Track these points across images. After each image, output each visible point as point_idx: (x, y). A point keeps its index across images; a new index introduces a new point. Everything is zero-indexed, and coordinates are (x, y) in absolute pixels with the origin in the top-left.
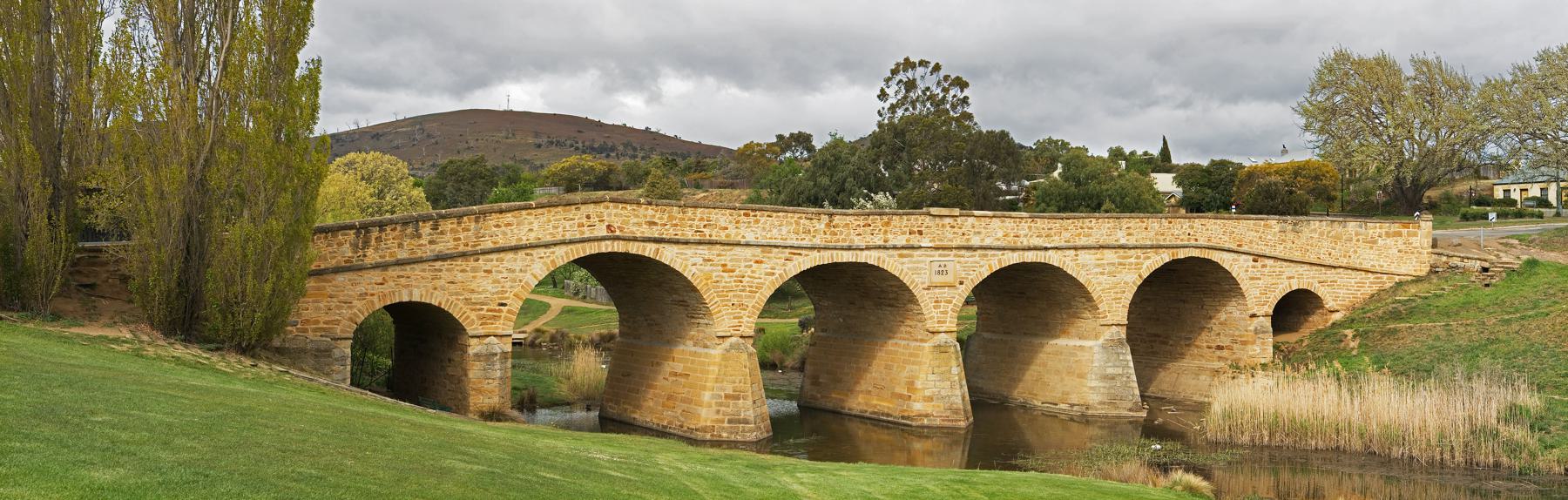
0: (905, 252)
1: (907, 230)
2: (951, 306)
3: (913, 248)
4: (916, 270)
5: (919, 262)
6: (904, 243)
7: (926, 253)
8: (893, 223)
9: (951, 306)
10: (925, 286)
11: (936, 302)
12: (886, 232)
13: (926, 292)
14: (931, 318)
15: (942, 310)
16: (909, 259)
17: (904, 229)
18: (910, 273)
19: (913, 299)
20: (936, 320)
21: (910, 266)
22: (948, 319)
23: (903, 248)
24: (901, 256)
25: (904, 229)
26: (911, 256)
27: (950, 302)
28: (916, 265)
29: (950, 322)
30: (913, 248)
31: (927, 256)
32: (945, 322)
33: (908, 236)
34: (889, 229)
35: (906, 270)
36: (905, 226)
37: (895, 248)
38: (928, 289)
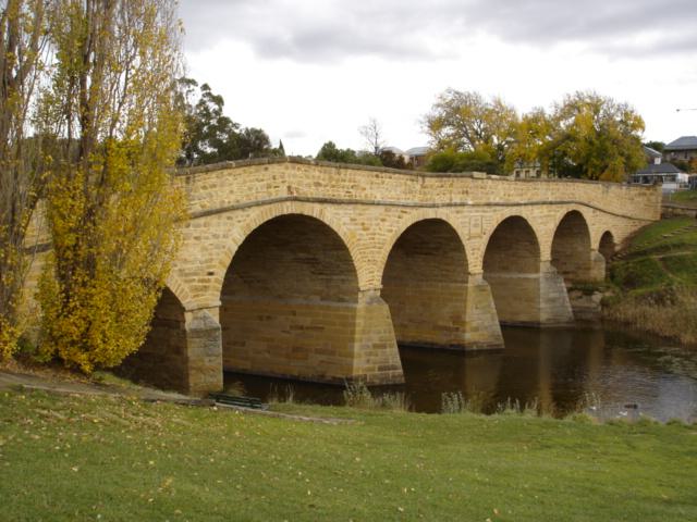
24: (458, 212)
26: (462, 212)
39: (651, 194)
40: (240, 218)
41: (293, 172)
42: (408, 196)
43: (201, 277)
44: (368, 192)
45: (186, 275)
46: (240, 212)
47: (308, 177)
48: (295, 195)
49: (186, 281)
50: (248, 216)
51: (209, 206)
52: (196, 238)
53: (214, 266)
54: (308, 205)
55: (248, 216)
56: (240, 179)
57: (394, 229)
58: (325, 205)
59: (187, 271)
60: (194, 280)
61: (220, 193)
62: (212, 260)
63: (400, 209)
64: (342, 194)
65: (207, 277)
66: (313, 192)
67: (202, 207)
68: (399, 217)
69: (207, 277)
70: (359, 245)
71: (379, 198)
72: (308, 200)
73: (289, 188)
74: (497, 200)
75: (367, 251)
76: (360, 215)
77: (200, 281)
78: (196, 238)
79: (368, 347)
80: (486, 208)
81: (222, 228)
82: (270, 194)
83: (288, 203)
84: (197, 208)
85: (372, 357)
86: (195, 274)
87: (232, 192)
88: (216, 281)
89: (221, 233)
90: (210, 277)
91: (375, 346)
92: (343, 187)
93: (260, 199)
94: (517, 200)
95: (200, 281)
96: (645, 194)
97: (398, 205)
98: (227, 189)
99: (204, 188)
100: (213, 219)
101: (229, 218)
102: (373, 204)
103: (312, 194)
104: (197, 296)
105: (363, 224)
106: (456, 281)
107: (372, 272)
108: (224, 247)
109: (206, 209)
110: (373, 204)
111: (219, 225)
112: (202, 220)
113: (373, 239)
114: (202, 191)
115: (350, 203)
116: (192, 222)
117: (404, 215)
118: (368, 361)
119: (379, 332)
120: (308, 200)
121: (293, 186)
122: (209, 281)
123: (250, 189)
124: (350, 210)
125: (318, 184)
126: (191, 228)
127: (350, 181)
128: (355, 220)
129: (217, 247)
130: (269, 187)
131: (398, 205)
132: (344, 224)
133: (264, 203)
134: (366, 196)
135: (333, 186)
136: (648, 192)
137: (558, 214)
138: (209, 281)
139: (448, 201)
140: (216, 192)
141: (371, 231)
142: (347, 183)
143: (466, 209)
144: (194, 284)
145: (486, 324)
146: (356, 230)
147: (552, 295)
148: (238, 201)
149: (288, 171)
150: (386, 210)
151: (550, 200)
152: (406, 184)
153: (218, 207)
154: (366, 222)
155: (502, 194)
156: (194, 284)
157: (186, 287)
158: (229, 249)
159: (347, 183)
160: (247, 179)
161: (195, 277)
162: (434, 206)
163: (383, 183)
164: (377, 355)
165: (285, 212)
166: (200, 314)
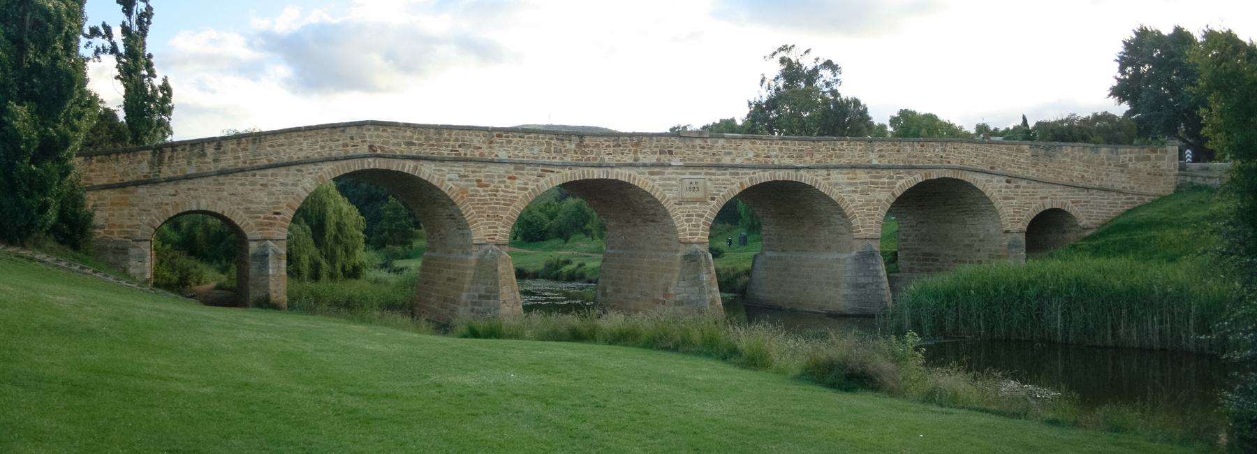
0: (657, 170)
1: (658, 150)
2: (703, 220)
3: (662, 166)
4: (667, 187)
5: (669, 179)
6: (654, 161)
7: (677, 171)
8: (643, 144)
9: (703, 220)
10: (676, 201)
11: (688, 216)
12: (636, 152)
13: (677, 207)
14: (683, 230)
15: (694, 223)
16: (660, 176)
17: (655, 149)
18: (661, 189)
19: (666, 214)
20: (688, 232)
21: (661, 182)
22: (700, 232)
23: (653, 165)
24: (651, 173)
25: (655, 149)
26: (663, 173)
27: (702, 216)
28: (667, 182)
29: (702, 234)
30: (662, 166)
31: (678, 174)
32: (697, 234)
33: (658, 155)
34: (639, 149)
35: (656, 186)
36: (655, 147)
37: (645, 165)
38: (680, 204)
39: (1158, 158)
40: (311, 171)
41: (376, 133)
42: (554, 155)
43: (268, 216)
44: (485, 149)
45: (252, 212)
46: (311, 168)
47: (395, 137)
48: (379, 152)
49: (251, 218)
50: (321, 169)
51: (275, 159)
52: (262, 185)
53: (282, 208)
54: (396, 161)
55: (321, 169)
56: (310, 140)
57: (530, 187)
58: (421, 162)
59: (252, 210)
60: (259, 217)
61: (287, 151)
62: (279, 203)
63: (540, 168)
64: (445, 152)
65: (273, 216)
66: (404, 149)
67: (269, 161)
68: (539, 176)
69: (273, 216)
70: (474, 200)
71: (503, 155)
72: (395, 157)
73: (371, 147)
74: (738, 161)
75: (486, 206)
76: (473, 172)
77: (265, 218)
78: (261, 185)
79: (474, 297)
80: (713, 171)
81: (291, 178)
82: (348, 152)
83: (370, 160)
84: (265, 162)
85: (476, 308)
86: (260, 212)
87: (301, 150)
88: (283, 219)
89: (290, 183)
90: (277, 216)
91: (480, 297)
92: (447, 146)
93: (334, 154)
94: (787, 161)
95: (265, 218)
96: (1148, 158)
97: (538, 165)
98: (297, 147)
99: (271, 146)
100: (283, 171)
101: (298, 171)
102: (492, 161)
103: (401, 151)
104: (263, 229)
105: (478, 181)
106: (672, 251)
107: (497, 228)
108: (293, 193)
109: (272, 163)
110: (492, 161)
111: (287, 175)
112: (270, 171)
113: (495, 195)
114: (269, 149)
115: (455, 160)
116: (258, 172)
117: (547, 174)
118: (472, 310)
119: (486, 284)
120: (395, 157)
121: (377, 145)
122: (275, 219)
123: (322, 147)
124: (460, 168)
125: (410, 144)
126: (257, 177)
127: (457, 140)
128: (465, 176)
129: (285, 193)
130: (345, 145)
131: (538, 165)
132: (450, 180)
133: (336, 159)
134: (481, 154)
135: (433, 145)
136: (1153, 156)
137: (901, 182)
138: (275, 219)
139: (631, 161)
140: (284, 150)
141: (491, 187)
142: (452, 143)
143: (670, 170)
144: (259, 220)
145: (693, 298)
146: (467, 186)
147: (861, 280)
148: (308, 157)
149: (370, 133)
150: (516, 169)
151: (875, 162)
152: (549, 144)
153: (286, 160)
154: (483, 179)
155: (751, 155)
156: (259, 220)
157: (251, 222)
158: (298, 195)
159: (452, 143)
160: (319, 140)
161: (262, 216)
162: (600, 166)
163: (510, 142)
164: (481, 305)
165: (366, 167)
166: (264, 243)
